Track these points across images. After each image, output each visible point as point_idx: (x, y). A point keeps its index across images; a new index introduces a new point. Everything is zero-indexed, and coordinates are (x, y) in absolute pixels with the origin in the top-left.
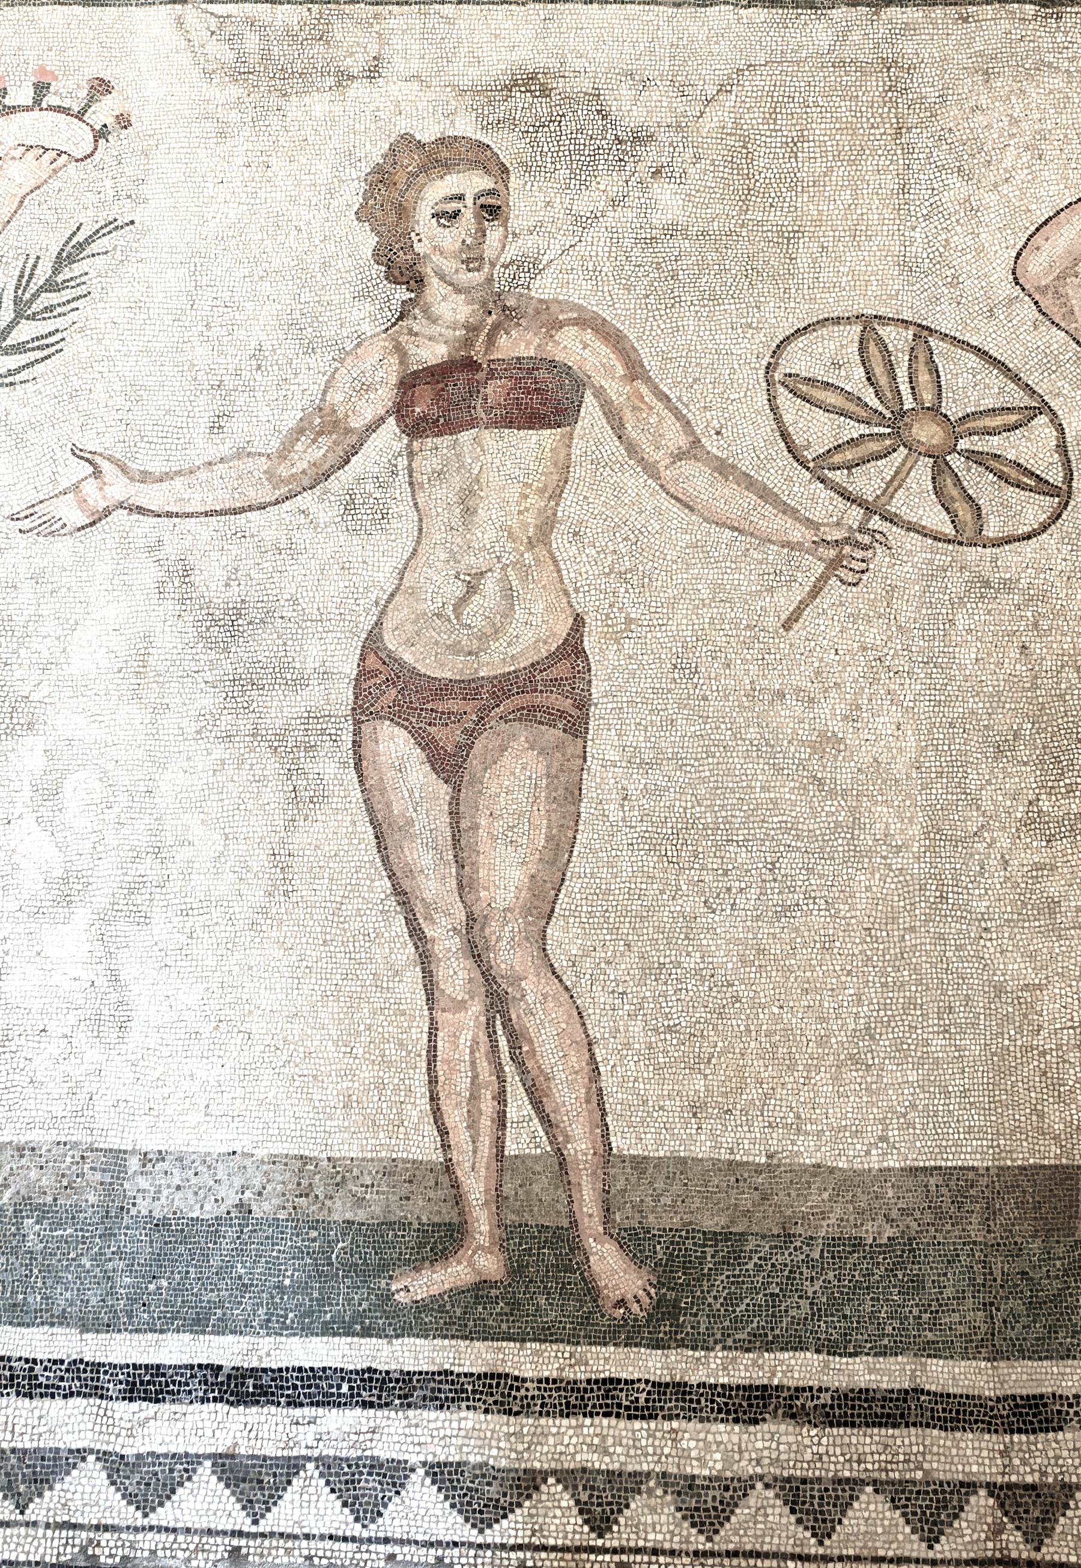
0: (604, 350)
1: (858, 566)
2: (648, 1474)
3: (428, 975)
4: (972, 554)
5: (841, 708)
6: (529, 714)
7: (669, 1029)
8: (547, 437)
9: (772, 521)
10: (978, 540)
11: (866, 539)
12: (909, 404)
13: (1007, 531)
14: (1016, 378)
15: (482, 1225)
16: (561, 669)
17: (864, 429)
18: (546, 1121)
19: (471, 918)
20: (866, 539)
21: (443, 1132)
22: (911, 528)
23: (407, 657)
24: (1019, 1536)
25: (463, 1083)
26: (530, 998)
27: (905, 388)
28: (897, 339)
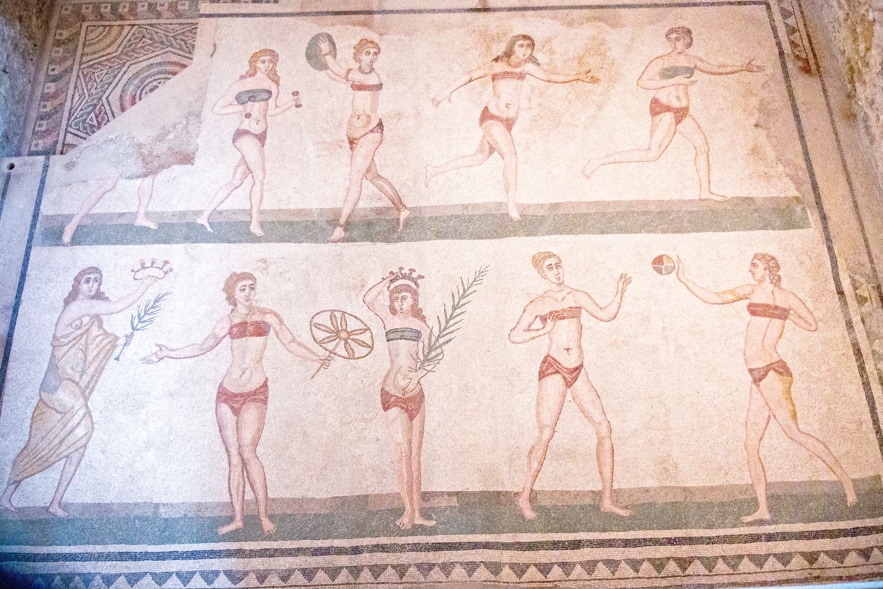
0: (275, 318)
1: (328, 365)
2: (272, 570)
3: (229, 460)
4: (352, 361)
5: (323, 396)
6: (254, 400)
7: (282, 469)
8: (262, 339)
9: (308, 355)
10: (354, 358)
11: (329, 359)
12: (340, 329)
13: (359, 356)
14: (363, 322)
15: (238, 517)
16: (262, 390)
17: (330, 335)
18: (254, 491)
19: (240, 446)
20: (329, 359)
21: (231, 495)
22: (339, 356)
23: (228, 388)
24: (352, 578)
25: (236, 485)
26: (252, 464)
27: (339, 326)
28: (338, 315)
